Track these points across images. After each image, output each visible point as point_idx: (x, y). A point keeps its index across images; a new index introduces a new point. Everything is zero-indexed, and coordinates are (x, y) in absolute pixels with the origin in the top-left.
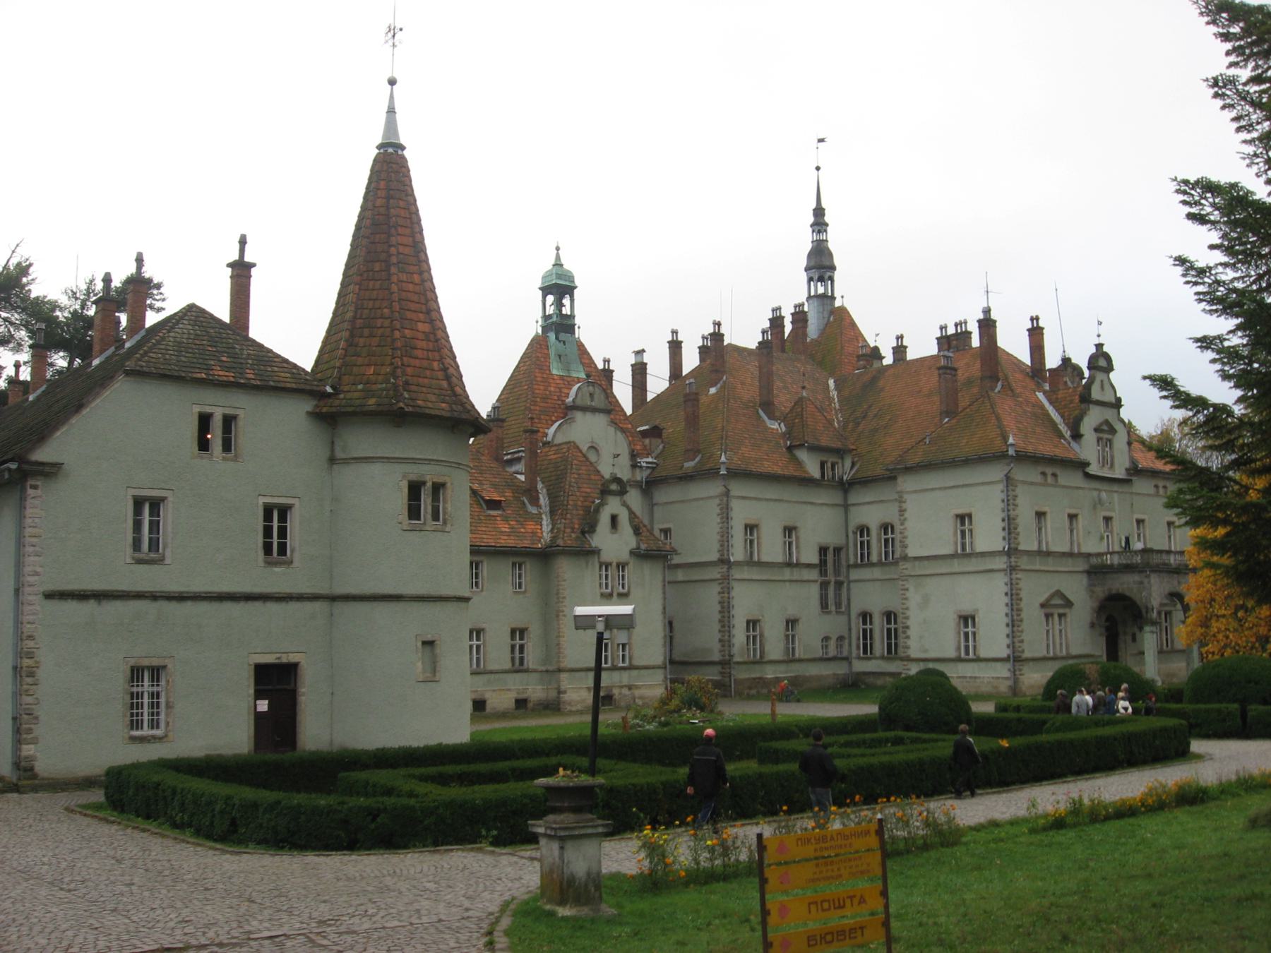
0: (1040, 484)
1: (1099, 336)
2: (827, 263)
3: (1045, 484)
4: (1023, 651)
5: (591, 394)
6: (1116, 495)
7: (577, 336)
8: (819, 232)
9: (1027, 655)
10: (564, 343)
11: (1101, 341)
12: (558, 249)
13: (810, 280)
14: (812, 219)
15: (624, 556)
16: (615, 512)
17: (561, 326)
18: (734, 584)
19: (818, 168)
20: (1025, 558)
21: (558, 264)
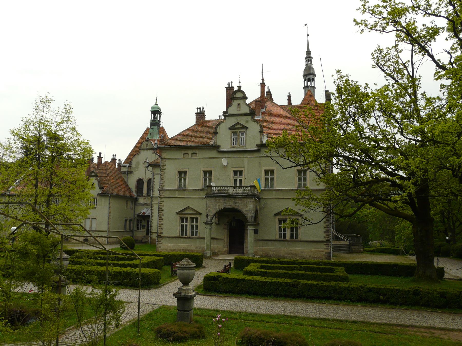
0: (182, 159)
1: (240, 82)
2: (311, 72)
3: (184, 158)
4: (162, 233)
5: (147, 144)
6: (246, 159)
7: (161, 126)
8: (309, 61)
9: (164, 234)
10: (153, 129)
11: (240, 85)
12: (157, 99)
13: (305, 80)
14: (305, 56)
15: (95, 196)
16: (93, 182)
17: (155, 123)
18: (153, 205)
19: (308, 35)
20: (168, 192)
21: (156, 104)
